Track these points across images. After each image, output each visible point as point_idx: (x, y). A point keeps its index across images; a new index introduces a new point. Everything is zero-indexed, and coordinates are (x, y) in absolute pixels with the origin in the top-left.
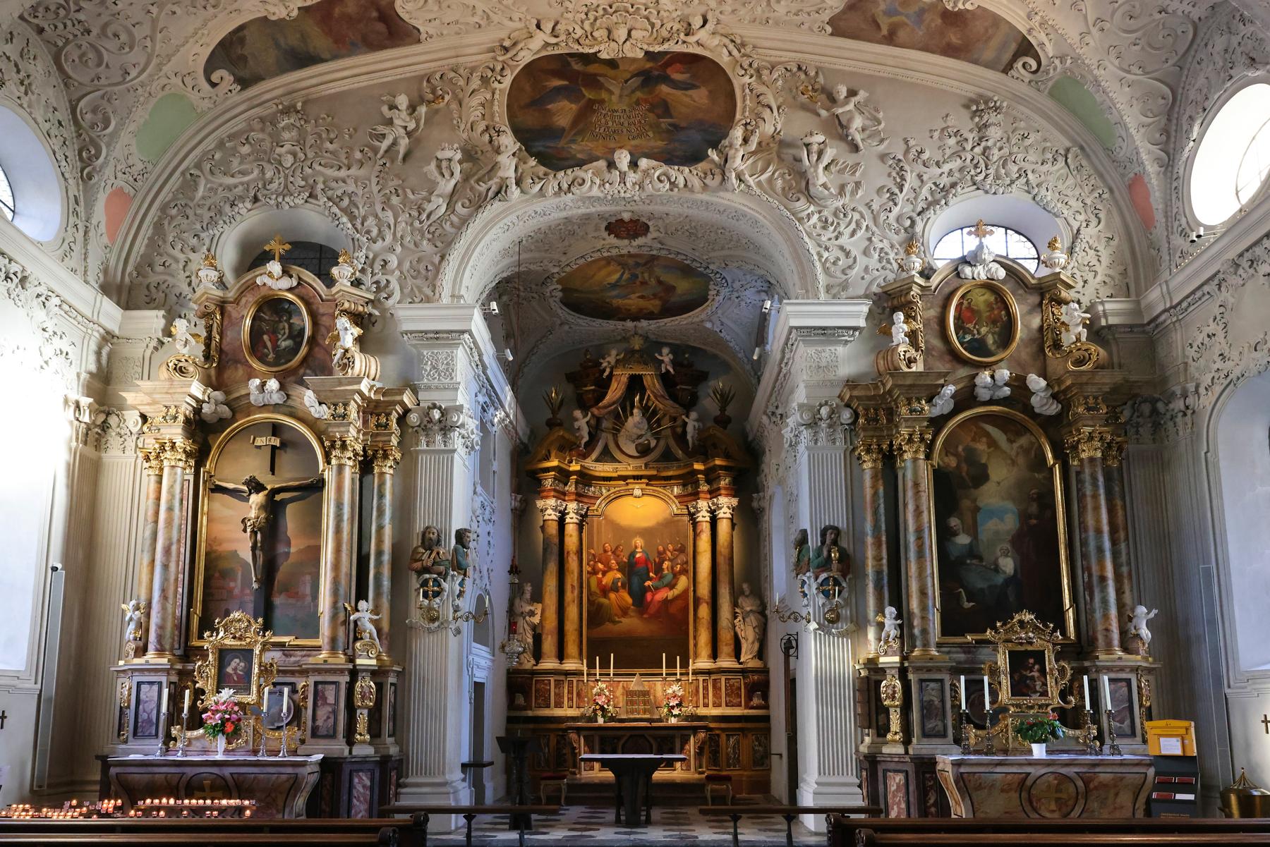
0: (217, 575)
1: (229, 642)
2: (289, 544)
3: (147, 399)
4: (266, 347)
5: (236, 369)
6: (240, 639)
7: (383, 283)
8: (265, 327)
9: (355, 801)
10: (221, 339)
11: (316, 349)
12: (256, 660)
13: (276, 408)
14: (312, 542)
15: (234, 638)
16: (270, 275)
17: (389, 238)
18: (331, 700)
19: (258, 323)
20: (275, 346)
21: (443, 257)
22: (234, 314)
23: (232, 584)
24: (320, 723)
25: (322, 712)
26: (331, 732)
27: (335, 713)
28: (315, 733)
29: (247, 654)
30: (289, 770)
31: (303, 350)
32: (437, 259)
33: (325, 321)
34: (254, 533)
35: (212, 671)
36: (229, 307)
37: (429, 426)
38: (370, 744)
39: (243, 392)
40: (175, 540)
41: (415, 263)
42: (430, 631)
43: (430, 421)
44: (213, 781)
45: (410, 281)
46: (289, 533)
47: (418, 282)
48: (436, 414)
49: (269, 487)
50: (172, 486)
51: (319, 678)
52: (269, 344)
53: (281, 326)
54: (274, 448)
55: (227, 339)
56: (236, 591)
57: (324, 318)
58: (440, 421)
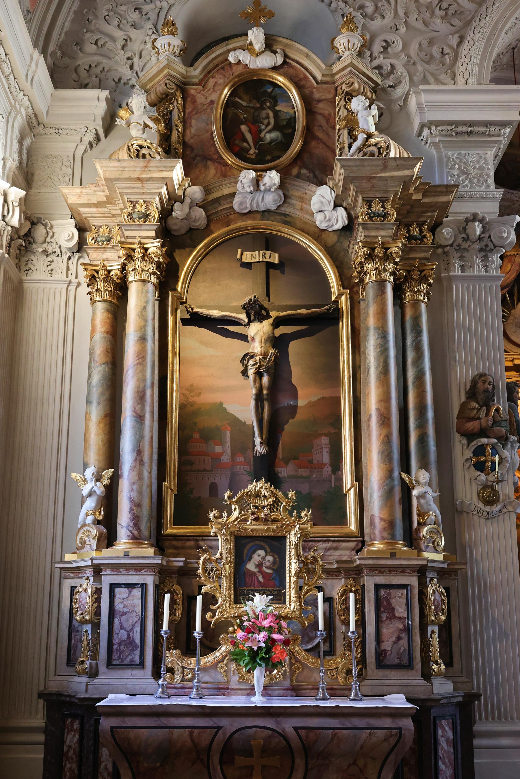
0: (197, 436)
1: (250, 526)
2: (295, 396)
3: (100, 194)
4: (245, 140)
5: (206, 167)
6: (265, 521)
7: (387, 68)
8: (243, 116)
9: (440, 763)
10: (184, 129)
11: (313, 143)
12: (291, 552)
13: (266, 213)
14: (327, 393)
15: (257, 519)
16: (249, 48)
17: (389, 15)
18: (401, 611)
19: (231, 111)
20: (257, 139)
21: (462, 39)
22: (200, 99)
23: (218, 449)
24: (387, 645)
25: (389, 631)
26: (406, 660)
27: (407, 630)
28: (382, 662)
29: (276, 544)
30: (387, 722)
31: (297, 145)
32: (454, 41)
33: (322, 108)
34: (259, 374)
35: (227, 569)
36: (192, 90)
37: (465, 245)
38: (446, 676)
39: (226, 191)
40: (149, 382)
41: (425, 45)
42: (489, 516)
43: (466, 239)
44: (267, 739)
45: (420, 67)
46: (294, 381)
47: (432, 67)
48: (478, 228)
49: (273, 314)
50: (145, 308)
51: (381, 580)
52: (249, 137)
53: (264, 113)
54: (269, 266)
55: (192, 131)
56: (226, 459)
57: (321, 105)
58: (480, 238)
